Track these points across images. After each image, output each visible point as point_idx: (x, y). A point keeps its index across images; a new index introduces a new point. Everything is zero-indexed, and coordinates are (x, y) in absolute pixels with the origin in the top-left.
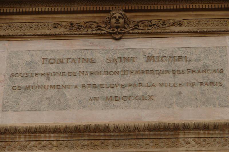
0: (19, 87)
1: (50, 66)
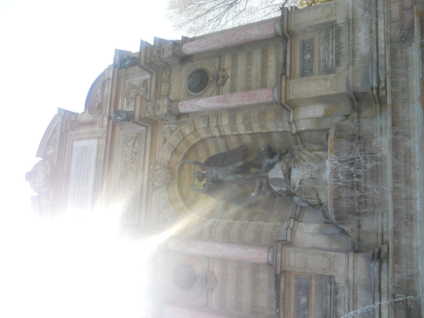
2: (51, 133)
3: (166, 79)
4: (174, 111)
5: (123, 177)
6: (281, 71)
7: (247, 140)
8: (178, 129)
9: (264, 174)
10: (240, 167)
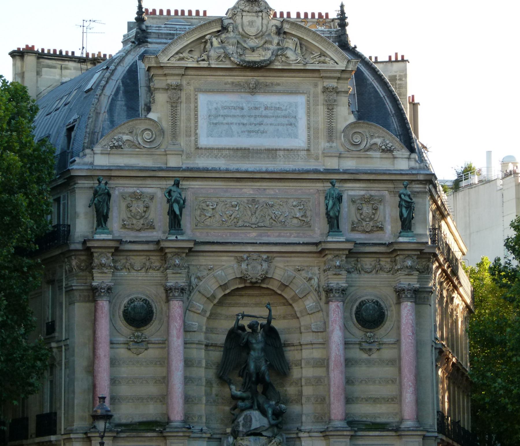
0: (213, 123)
1: (225, 111)
2: (320, 47)
3: (379, 266)
4: (332, 296)
5: (252, 205)
6: (367, 420)
7: (295, 373)
8: (311, 288)
9: (256, 404)
10: (263, 378)
